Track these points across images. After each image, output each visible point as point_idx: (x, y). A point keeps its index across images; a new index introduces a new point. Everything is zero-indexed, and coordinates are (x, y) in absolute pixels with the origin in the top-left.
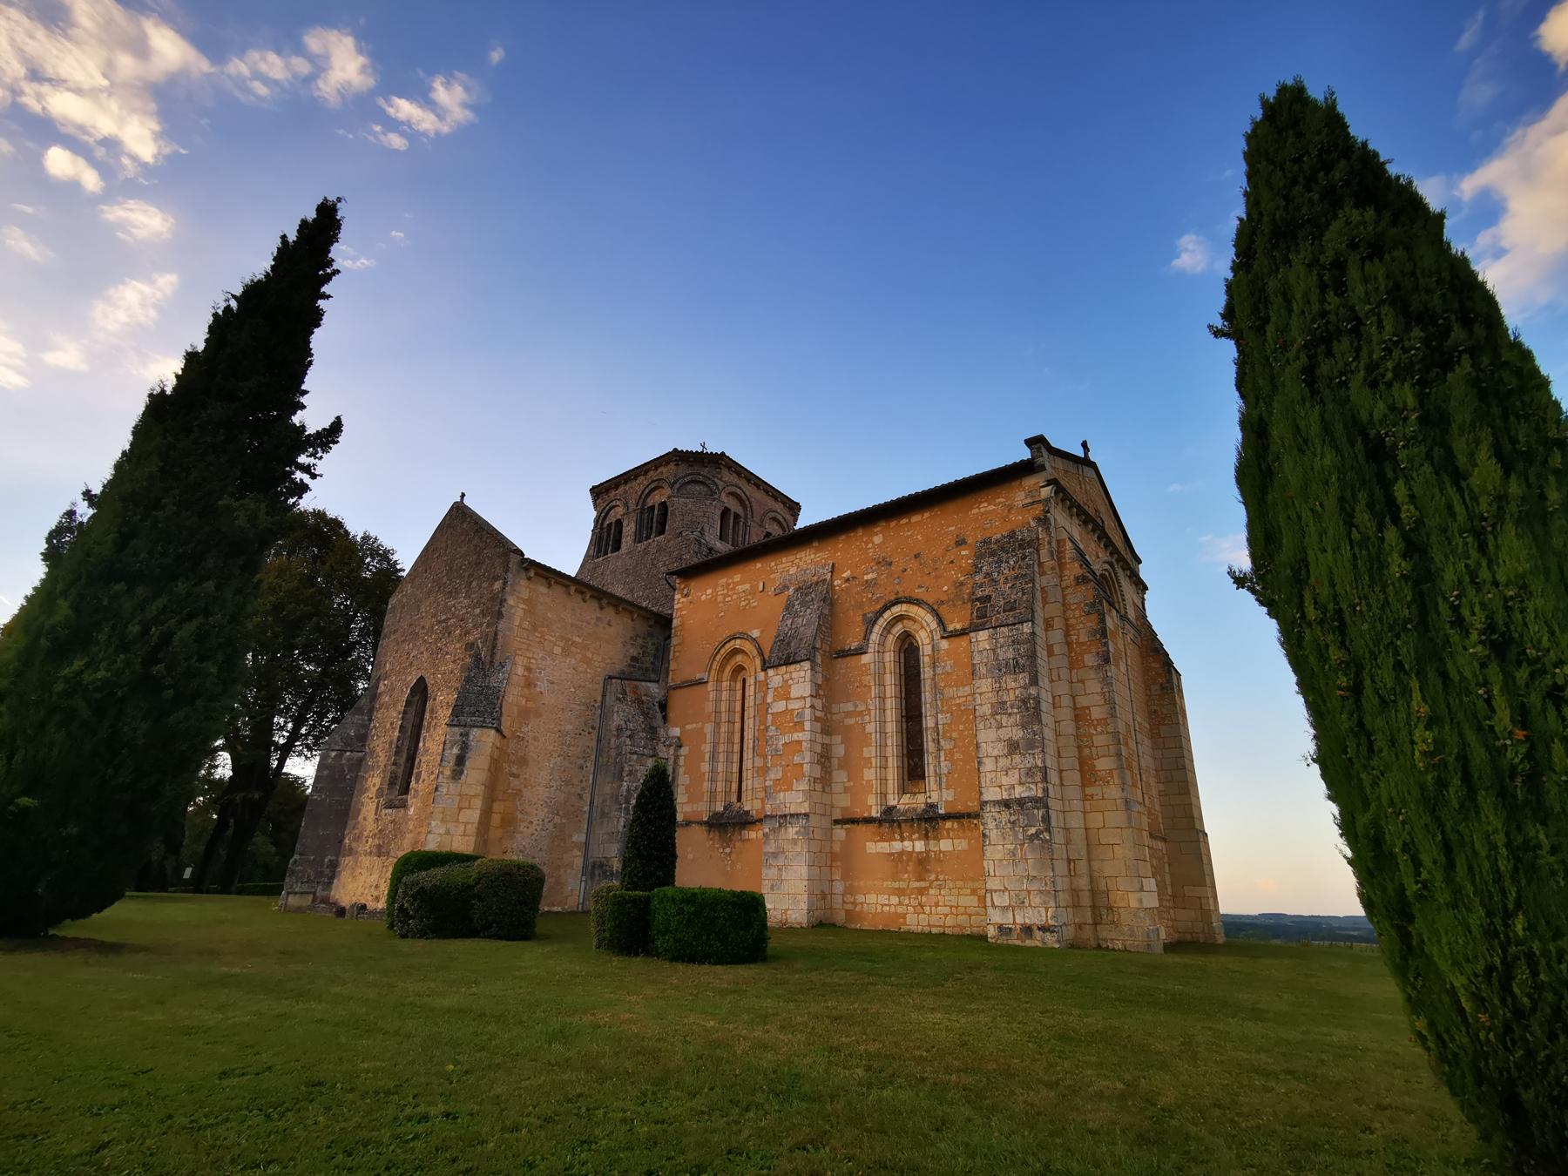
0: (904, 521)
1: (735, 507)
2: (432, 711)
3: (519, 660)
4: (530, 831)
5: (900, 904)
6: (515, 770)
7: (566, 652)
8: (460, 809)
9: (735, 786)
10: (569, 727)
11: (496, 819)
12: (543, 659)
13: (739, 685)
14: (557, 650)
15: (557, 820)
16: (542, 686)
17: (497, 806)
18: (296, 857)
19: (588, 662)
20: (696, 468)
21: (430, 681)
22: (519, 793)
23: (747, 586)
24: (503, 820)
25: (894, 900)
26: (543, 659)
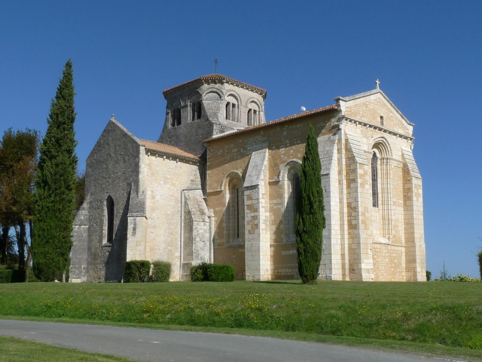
0: (294, 126)
1: (232, 100)
2: (117, 210)
3: (148, 189)
4: (160, 252)
5: (292, 272)
6: (152, 230)
7: (165, 182)
8: (137, 246)
9: (236, 232)
10: (169, 212)
11: (148, 249)
12: (157, 187)
13: (236, 192)
14: (162, 182)
15: (169, 248)
16: (158, 198)
17: (148, 244)
18: (71, 266)
19: (173, 185)
20: (212, 85)
21: (114, 198)
22: (154, 239)
23: (236, 150)
24: (150, 249)
25: (291, 270)
26: (157, 187)
